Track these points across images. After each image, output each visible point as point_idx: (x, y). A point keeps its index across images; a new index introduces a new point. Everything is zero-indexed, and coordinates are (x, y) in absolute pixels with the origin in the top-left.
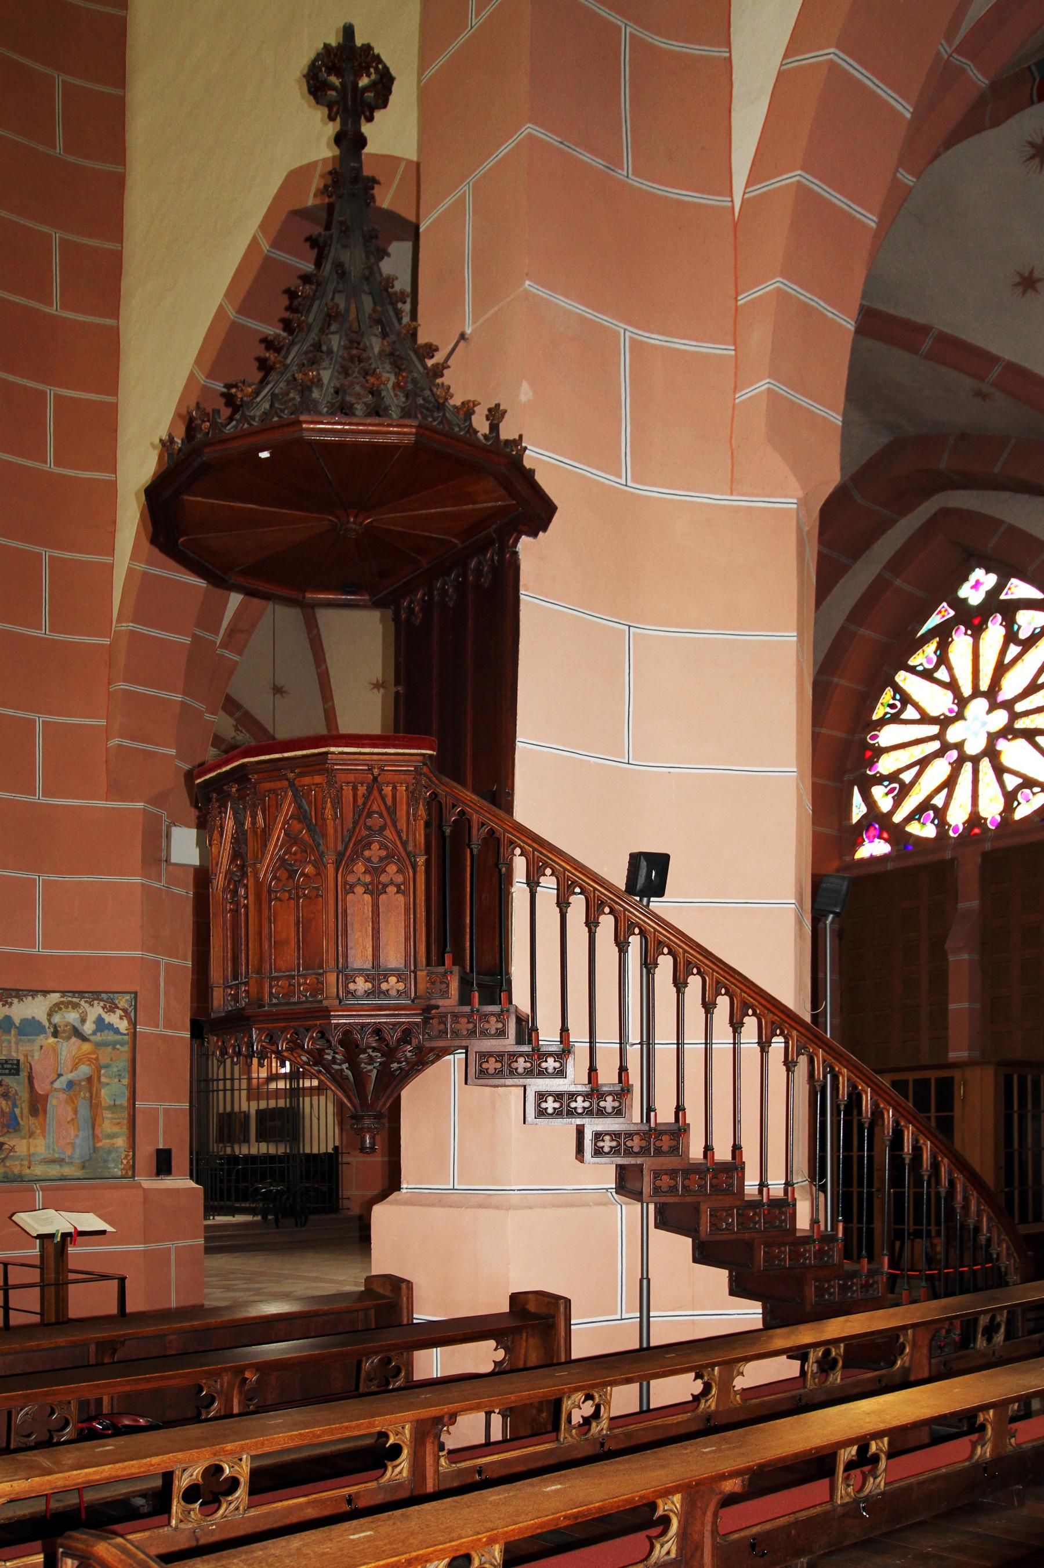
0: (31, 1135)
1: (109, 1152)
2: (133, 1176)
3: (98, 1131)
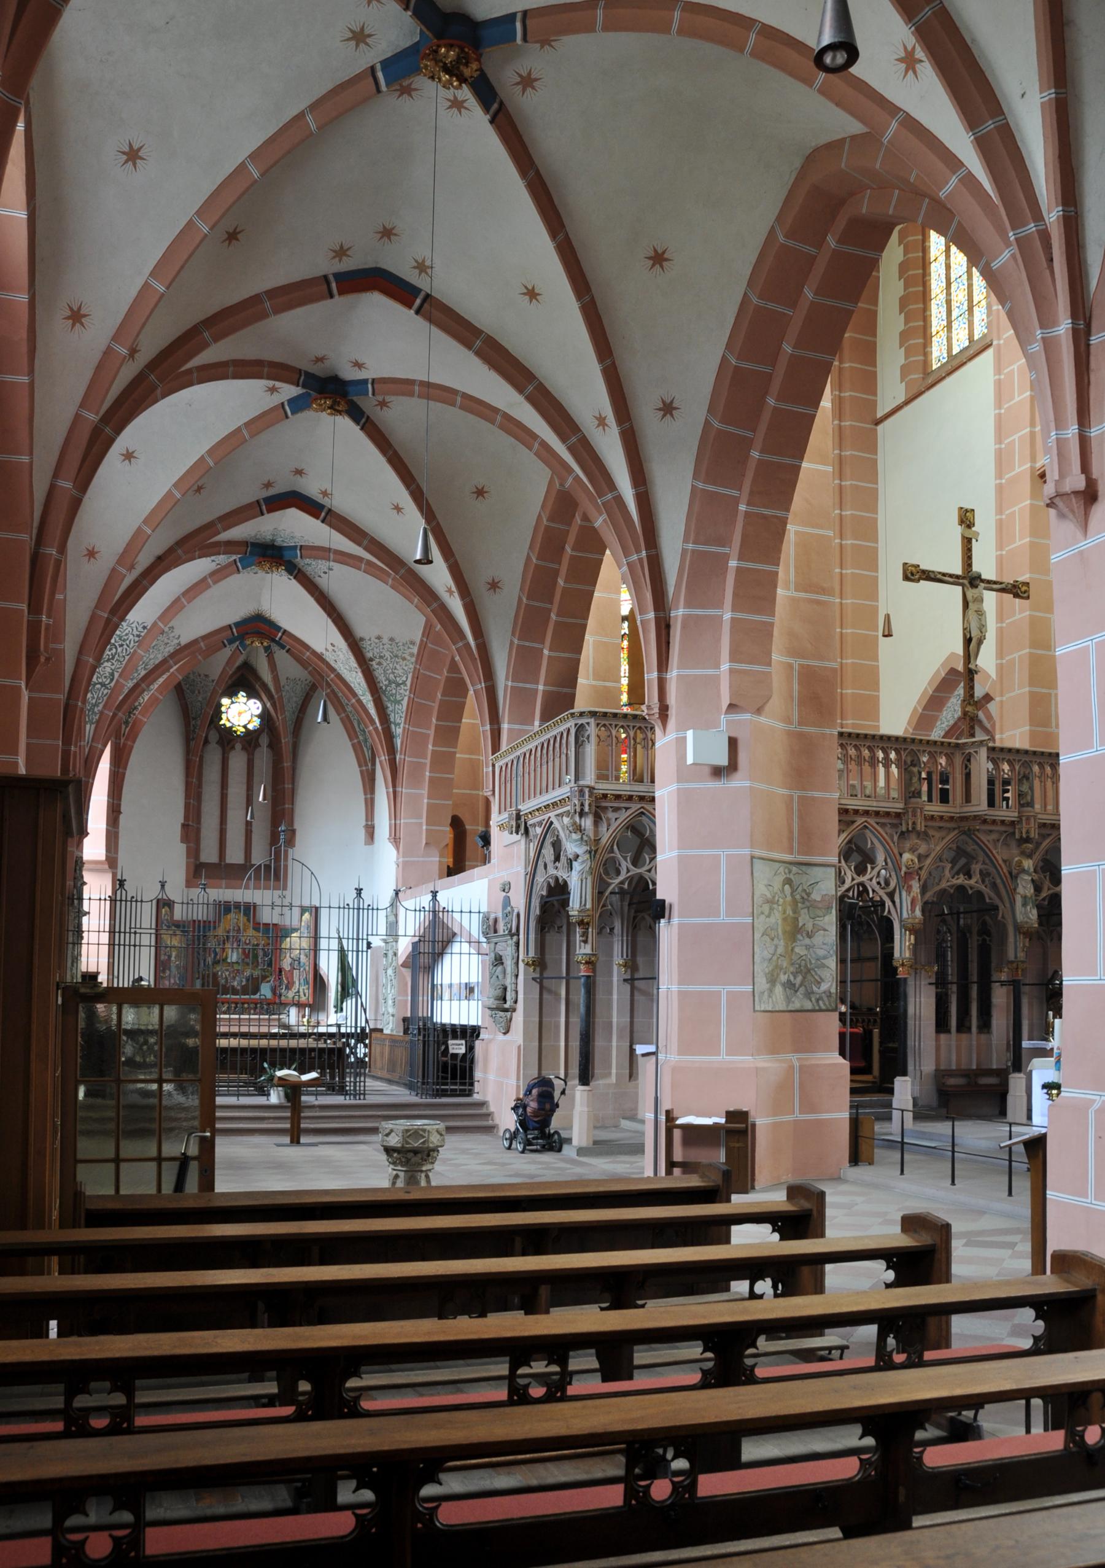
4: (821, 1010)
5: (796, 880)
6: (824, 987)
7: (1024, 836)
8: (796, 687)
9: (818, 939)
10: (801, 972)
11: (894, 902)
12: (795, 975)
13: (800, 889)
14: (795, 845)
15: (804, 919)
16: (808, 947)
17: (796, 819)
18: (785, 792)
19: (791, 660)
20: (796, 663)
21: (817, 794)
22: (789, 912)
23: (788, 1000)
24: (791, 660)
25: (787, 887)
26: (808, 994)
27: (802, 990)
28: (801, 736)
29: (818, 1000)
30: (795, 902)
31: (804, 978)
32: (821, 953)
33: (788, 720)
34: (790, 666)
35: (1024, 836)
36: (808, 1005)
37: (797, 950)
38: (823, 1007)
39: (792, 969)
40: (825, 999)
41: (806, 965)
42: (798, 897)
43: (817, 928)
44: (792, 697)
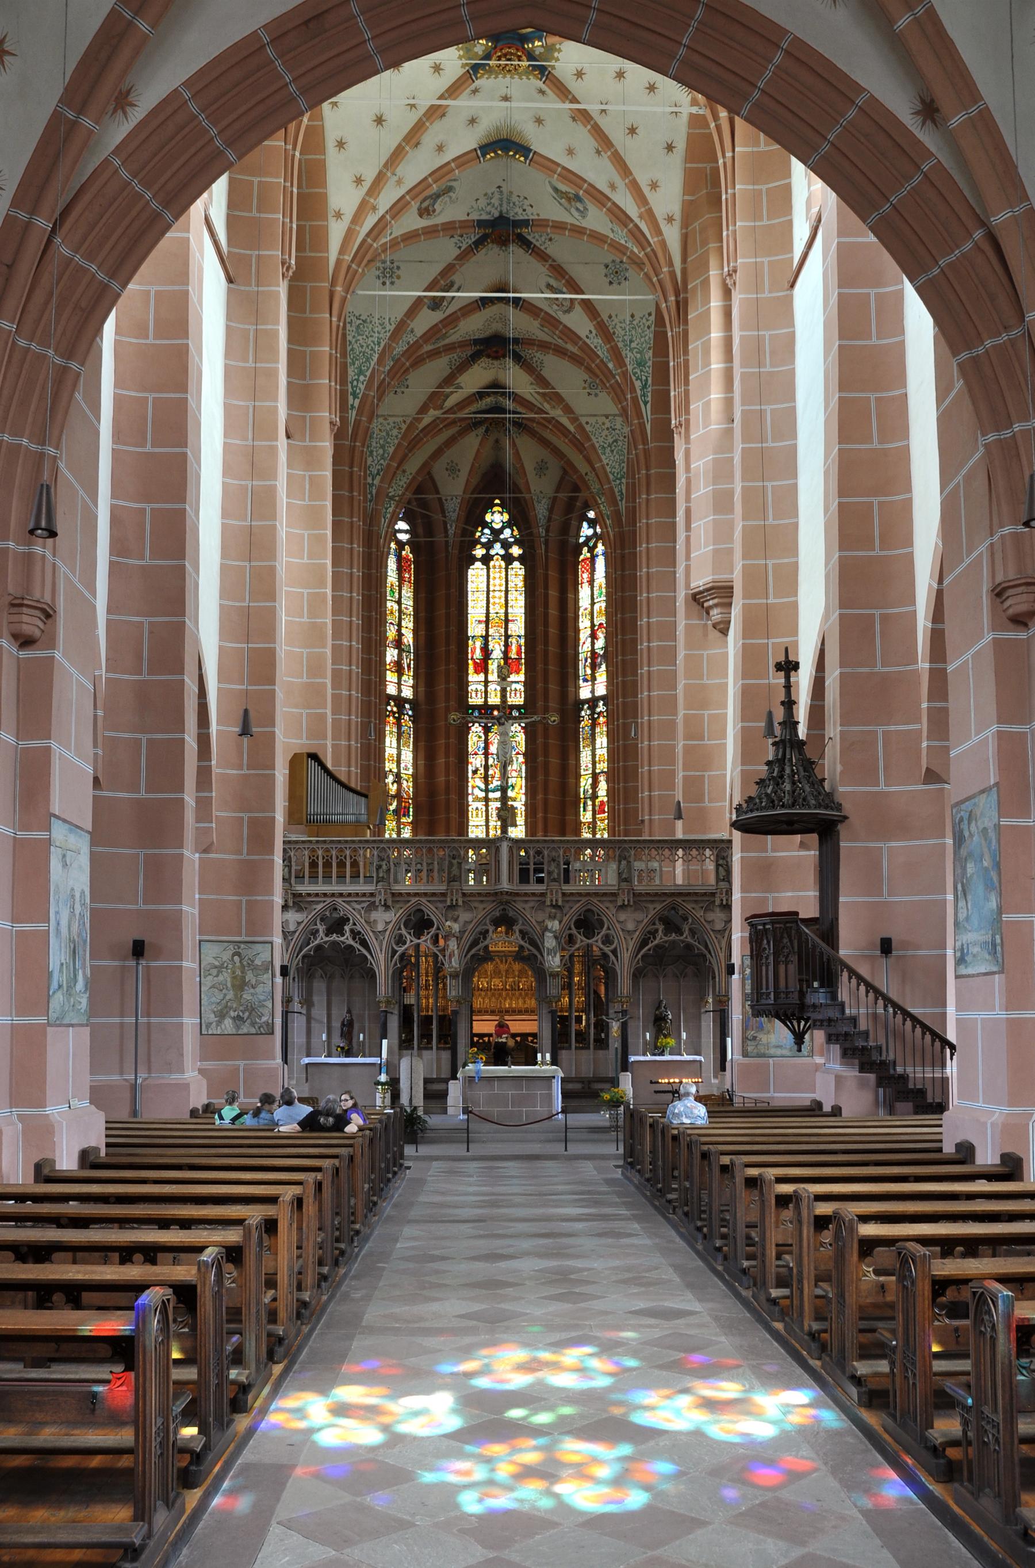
0: (769, 1032)
5: (243, 953)
6: (264, 1019)
9: (259, 989)
14: (244, 931)
15: (250, 976)
16: (253, 995)
17: (244, 915)
20: (245, 816)
21: (259, 898)
22: (238, 972)
23: (238, 1027)
24: (241, 815)
25: (236, 958)
26: (253, 1024)
27: (249, 1021)
30: (243, 966)
32: (262, 998)
36: (253, 1031)
43: (258, 982)
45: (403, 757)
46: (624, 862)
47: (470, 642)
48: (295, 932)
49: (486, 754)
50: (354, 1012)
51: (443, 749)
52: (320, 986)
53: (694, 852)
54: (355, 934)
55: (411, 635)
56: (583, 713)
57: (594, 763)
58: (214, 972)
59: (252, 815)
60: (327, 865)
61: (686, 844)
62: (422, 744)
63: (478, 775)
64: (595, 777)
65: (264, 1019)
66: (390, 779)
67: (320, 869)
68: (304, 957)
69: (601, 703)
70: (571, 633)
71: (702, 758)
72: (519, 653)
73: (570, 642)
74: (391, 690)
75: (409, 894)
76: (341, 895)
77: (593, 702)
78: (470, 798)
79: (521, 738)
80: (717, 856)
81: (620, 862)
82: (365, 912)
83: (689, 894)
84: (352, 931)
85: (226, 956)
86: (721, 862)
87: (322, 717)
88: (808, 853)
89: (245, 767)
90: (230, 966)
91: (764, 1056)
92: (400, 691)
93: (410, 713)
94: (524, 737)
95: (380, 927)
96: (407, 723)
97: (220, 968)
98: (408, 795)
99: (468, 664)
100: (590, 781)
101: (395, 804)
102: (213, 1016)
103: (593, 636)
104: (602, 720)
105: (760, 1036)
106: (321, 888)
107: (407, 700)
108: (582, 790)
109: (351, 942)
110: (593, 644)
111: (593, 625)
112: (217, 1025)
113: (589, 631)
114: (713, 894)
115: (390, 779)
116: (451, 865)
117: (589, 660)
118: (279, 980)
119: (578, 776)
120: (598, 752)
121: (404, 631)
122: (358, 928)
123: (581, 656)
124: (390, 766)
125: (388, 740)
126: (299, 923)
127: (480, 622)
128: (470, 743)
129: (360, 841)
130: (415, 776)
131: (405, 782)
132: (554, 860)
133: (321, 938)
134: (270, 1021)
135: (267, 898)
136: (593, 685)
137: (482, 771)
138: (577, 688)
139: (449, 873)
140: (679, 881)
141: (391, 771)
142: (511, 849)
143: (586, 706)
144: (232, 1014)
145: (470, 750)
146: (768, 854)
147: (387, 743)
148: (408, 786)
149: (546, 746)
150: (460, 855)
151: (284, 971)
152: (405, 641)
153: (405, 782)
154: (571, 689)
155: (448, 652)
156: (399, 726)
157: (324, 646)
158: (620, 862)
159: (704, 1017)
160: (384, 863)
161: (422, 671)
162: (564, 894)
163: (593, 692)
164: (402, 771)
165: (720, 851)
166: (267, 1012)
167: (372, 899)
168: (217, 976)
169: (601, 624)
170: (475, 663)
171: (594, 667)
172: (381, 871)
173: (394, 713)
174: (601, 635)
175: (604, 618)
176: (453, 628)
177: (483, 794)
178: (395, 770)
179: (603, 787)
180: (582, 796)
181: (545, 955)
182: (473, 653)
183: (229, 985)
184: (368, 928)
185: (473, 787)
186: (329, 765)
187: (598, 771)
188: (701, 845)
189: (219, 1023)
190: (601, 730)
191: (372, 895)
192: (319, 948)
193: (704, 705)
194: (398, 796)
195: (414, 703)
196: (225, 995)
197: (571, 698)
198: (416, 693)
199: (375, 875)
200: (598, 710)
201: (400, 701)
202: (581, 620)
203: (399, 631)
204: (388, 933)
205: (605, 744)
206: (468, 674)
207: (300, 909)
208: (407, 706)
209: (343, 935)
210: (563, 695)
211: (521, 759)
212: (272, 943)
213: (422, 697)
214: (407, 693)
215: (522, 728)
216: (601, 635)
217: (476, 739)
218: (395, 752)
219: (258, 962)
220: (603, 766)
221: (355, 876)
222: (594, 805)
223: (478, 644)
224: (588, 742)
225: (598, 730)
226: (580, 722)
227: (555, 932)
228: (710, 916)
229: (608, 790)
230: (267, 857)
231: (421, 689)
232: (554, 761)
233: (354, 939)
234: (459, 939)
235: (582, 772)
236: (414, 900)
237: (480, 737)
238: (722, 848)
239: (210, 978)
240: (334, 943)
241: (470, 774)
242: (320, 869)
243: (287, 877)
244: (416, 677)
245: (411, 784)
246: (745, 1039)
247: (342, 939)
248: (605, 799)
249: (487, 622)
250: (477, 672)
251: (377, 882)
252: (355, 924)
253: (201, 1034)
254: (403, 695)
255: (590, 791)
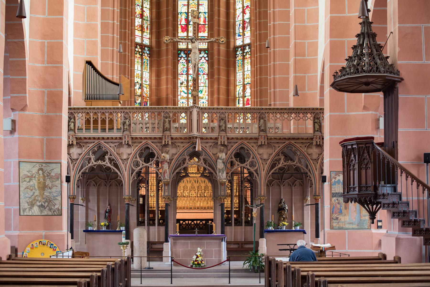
0: (345, 215)
1: (364, 221)
2: (370, 229)
3: (361, 214)
4: (55, 215)
5: (45, 169)
6: (56, 207)
7: (223, 144)
8: (46, 99)
9: (54, 190)
10: (47, 202)
11: (258, 174)
12: (45, 203)
13: (46, 172)
14: (45, 156)
15: (48, 182)
16: (50, 193)
17: (45, 147)
18: (40, 137)
19: (43, 90)
20: (46, 90)
22: (42, 180)
23: (41, 211)
24: (43, 90)
26: (50, 210)
27: (48, 208)
28: (47, 117)
29: (54, 212)
30: (44, 176)
31: (49, 204)
32: (55, 194)
33: (42, 111)
34: (44, 92)
35: (223, 144)
36: (50, 213)
37: (45, 194)
38: (56, 214)
39: (43, 200)
40: (57, 211)
41: (49, 199)
42: (45, 175)
43: (53, 186)
44: (44, 103)
45: (144, 75)
46: (262, 121)
47: (179, 16)
48: (78, 159)
49: (188, 74)
50: (112, 205)
51: (165, 71)
52: (93, 190)
53: (301, 115)
54: (111, 160)
55: (149, 12)
56: (238, 53)
57: (244, 79)
58: (28, 179)
59: (49, 90)
60: (96, 122)
61: (297, 111)
62: (154, 69)
63: (183, 85)
64: (244, 86)
65: (56, 207)
66: (137, 86)
67: (92, 125)
68: (82, 173)
69: (247, 47)
70: (232, 11)
71: (304, 66)
72: (205, 21)
73: (232, 16)
74: (138, 40)
75: (141, 138)
76: (103, 138)
77: (243, 47)
78: (179, 97)
79: (206, 66)
80: (314, 117)
81: (260, 120)
82: (117, 148)
83: (298, 139)
84: (109, 159)
85: (35, 170)
86: (316, 121)
87: (95, 43)
88: (368, 112)
89: (46, 62)
90: (37, 176)
91: (342, 228)
92: (142, 40)
93: (148, 52)
94: (207, 65)
95: (125, 157)
96: (146, 57)
97: (31, 178)
98: (147, 95)
99: (178, 27)
100: (242, 88)
101: (140, 99)
102: (27, 205)
103: (244, 12)
104: (248, 56)
105: (340, 217)
106: (92, 134)
107: (146, 46)
108: (237, 93)
109: (109, 165)
110: (243, 16)
111: (243, 7)
112: (29, 210)
113: (241, 10)
114: (312, 139)
115: (137, 86)
116: (164, 122)
117: (241, 25)
118: (65, 184)
119: (235, 86)
120: (246, 73)
121: (144, 9)
122: (113, 157)
123: (237, 23)
124: (137, 80)
125: (136, 66)
126: (80, 154)
127: (184, 5)
128: (179, 68)
129: (114, 108)
130: (150, 86)
131: (145, 89)
132: (223, 119)
133: (93, 163)
134: (60, 208)
135: (58, 137)
136: (243, 38)
137: (185, 83)
138: (235, 40)
139: (164, 126)
140: (292, 132)
141: (137, 82)
142: (198, 113)
143: (239, 49)
144: (38, 204)
145: (179, 72)
146: (345, 114)
147: (136, 68)
148: (146, 90)
149: (219, 70)
150: (170, 117)
151: (68, 179)
152: (145, 14)
153: (145, 89)
154: (232, 40)
155: (167, 21)
156: (142, 59)
157: (96, 4)
158: (260, 120)
159: (305, 208)
160: (127, 121)
161: (154, 30)
162: (228, 138)
163: (243, 41)
164: (144, 83)
165: (315, 115)
166: (58, 202)
167: (120, 141)
168: (29, 182)
169: (247, 6)
170: (182, 27)
171: (244, 28)
172: (125, 125)
173: (140, 52)
174: (248, 11)
175: (249, 3)
176: (171, 8)
177: (186, 95)
178: (140, 82)
179: (248, 91)
180: (237, 96)
181: (218, 173)
182: (181, 21)
183: (36, 187)
184: (118, 157)
185: (181, 92)
186: (99, 69)
187: (245, 83)
188: (305, 111)
189: (30, 209)
190: (248, 62)
191: (120, 138)
192: (92, 169)
193: (305, 37)
194: (141, 96)
195: (150, 48)
196: (34, 193)
197: (232, 46)
198: (151, 42)
199: (122, 128)
200: (246, 51)
201: (142, 46)
202: (237, 4)
203: (142, 9)
204: (129, 160)
205: (249, 69)
206: (178, 33)
207: (81, 147)
208: (146, 49)
209: (104, 161)
210: (228, 43)
211: (206, 77)
212: (61, 163)
213: (154, 44)
214: (147, 42)
215: (207, 61)
216: (248, 11)
217: (182, 66)
218: (140, 72)
219: (53, 174)
220: (248, 81)
221: (111, 129)
222: (243, 101)
223: (184, 16)
224: (241, 68)
225: (246, 61)
226: (236, 58)
227: (223, 159)
228: (310, 151)
229: (251, 93)
230: (58, 114)
231: (154, 40)
232: (223, 77)
233: (110, 163)
234: (169, 163)
235: (238, 84)
236: (144, 141)
237: (184, 65)
238: (317, 114)
239: (25, 183)
240: (100, 166)
241: (179, 85)
242: (92, 125)
243: (73, 128)
244: (151, 33)
245: (148, 90)
246: (331, 219)
247: (104, 163)
248: (250, 98)
249: (188, 5)
250: (183, 31)
251: (123, 131)
252: (111, 155)
253: (20, 215)
254: (144, 43)
255: (242, 93)
